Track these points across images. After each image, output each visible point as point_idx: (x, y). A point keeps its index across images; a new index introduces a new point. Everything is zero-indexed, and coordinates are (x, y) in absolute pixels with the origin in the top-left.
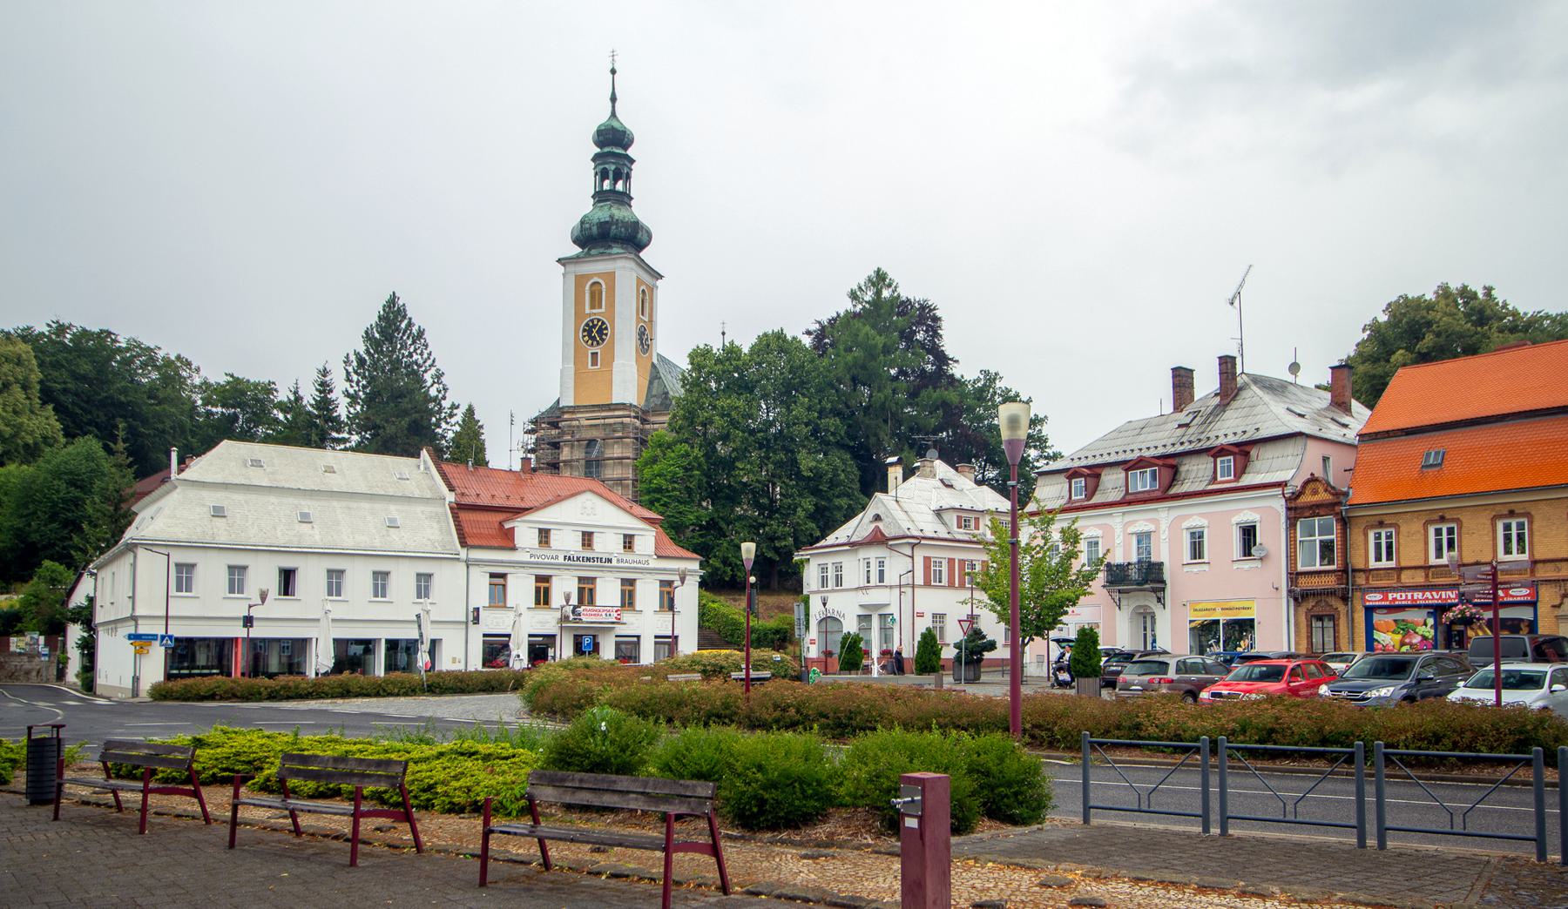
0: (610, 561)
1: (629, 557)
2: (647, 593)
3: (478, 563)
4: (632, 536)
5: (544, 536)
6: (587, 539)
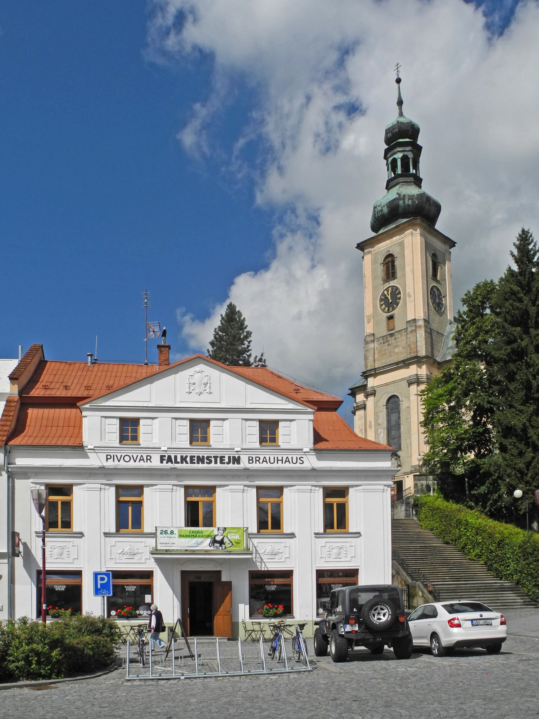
0: (237, 460)
1: (269, 453)
2: (302, 506)
3: (27, 473)
4: (275, 423)
5: (129, 429)
6: (199, 429)
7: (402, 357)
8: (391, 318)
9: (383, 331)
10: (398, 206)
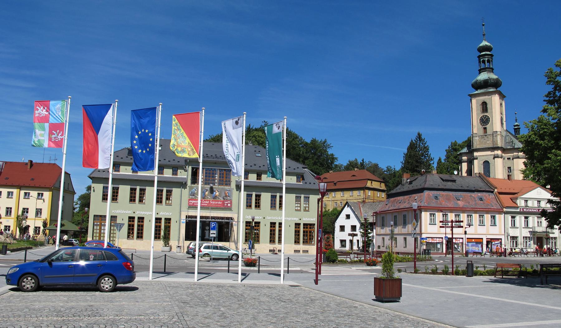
5: (526, 201)
7: (491, 146)
8: (485, 129)
9: (481, 132)
10: (488, 82)
